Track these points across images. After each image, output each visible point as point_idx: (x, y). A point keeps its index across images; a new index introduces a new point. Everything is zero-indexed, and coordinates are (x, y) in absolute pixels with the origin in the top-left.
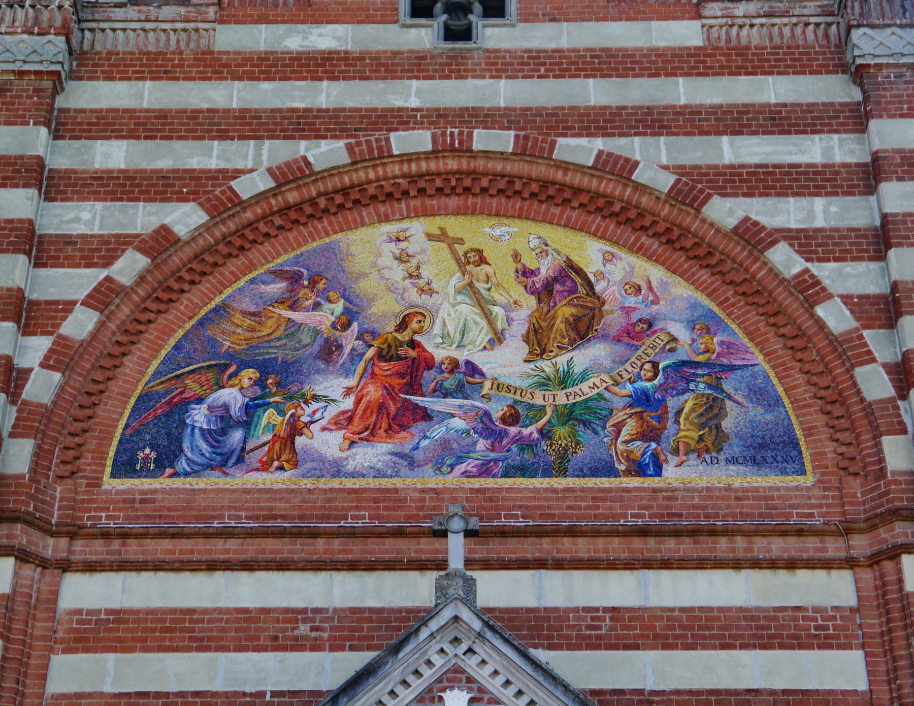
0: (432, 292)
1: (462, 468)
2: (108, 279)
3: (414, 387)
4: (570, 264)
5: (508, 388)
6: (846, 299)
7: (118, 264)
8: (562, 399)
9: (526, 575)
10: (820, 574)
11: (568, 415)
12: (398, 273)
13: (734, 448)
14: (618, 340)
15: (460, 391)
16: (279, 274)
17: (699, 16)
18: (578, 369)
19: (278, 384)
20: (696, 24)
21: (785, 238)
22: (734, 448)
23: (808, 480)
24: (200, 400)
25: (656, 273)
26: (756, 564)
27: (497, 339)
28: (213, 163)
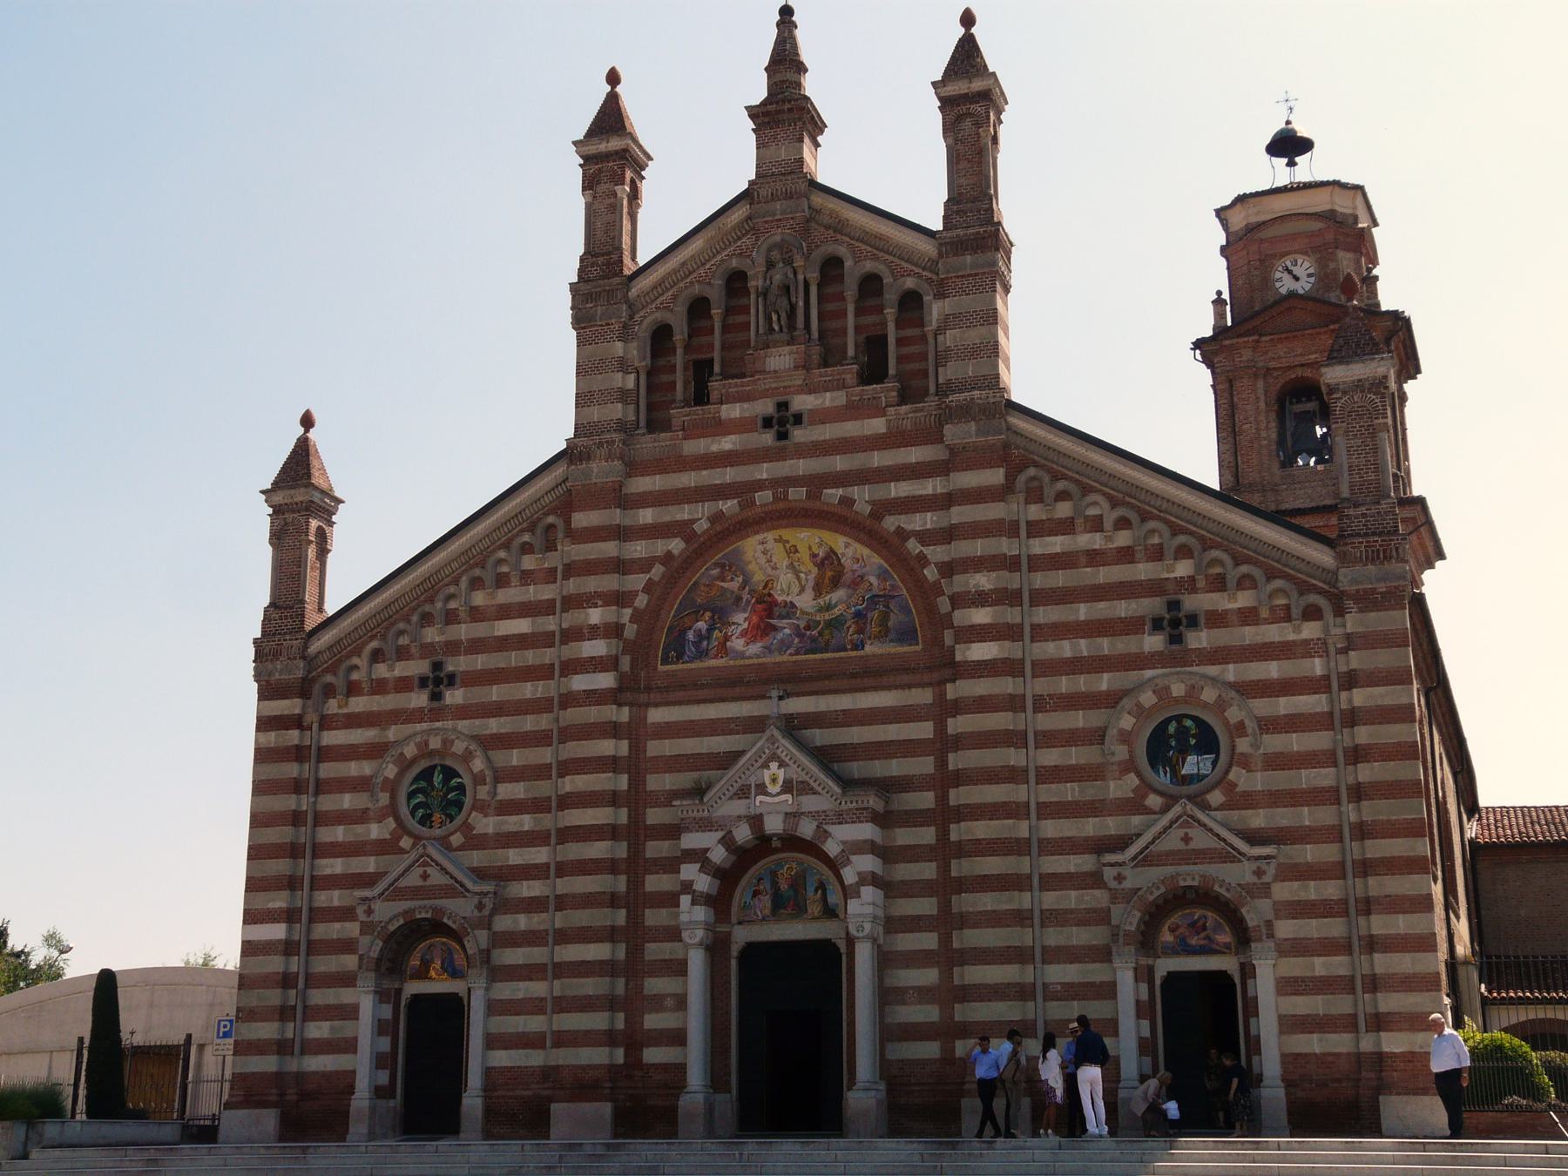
0: (776, 569)
1: (789, 652)
2: (650, 578)
3: (770, 616)
4: (832, 551)
5: (807, 614)
6: (936, 564)
7: (654, 570)
8: (827, 617)
9: (812, 698)
10: (920, 690)
11: (830, 624)
12: (763, 560)
13: (892, 635)
14: (849, 587)
15: (788, 616)
16: (716, 565)
17: (884, 415)
18: (833, 602)
19: (719, 618)
20: (883, 420)
21: (914, 535)
22: (892, 635)
23: (920, 646)
24: (690, 628)
25: (866, 551)
26: (896, 687)
27: (802, 589)
28: (686, 517)
